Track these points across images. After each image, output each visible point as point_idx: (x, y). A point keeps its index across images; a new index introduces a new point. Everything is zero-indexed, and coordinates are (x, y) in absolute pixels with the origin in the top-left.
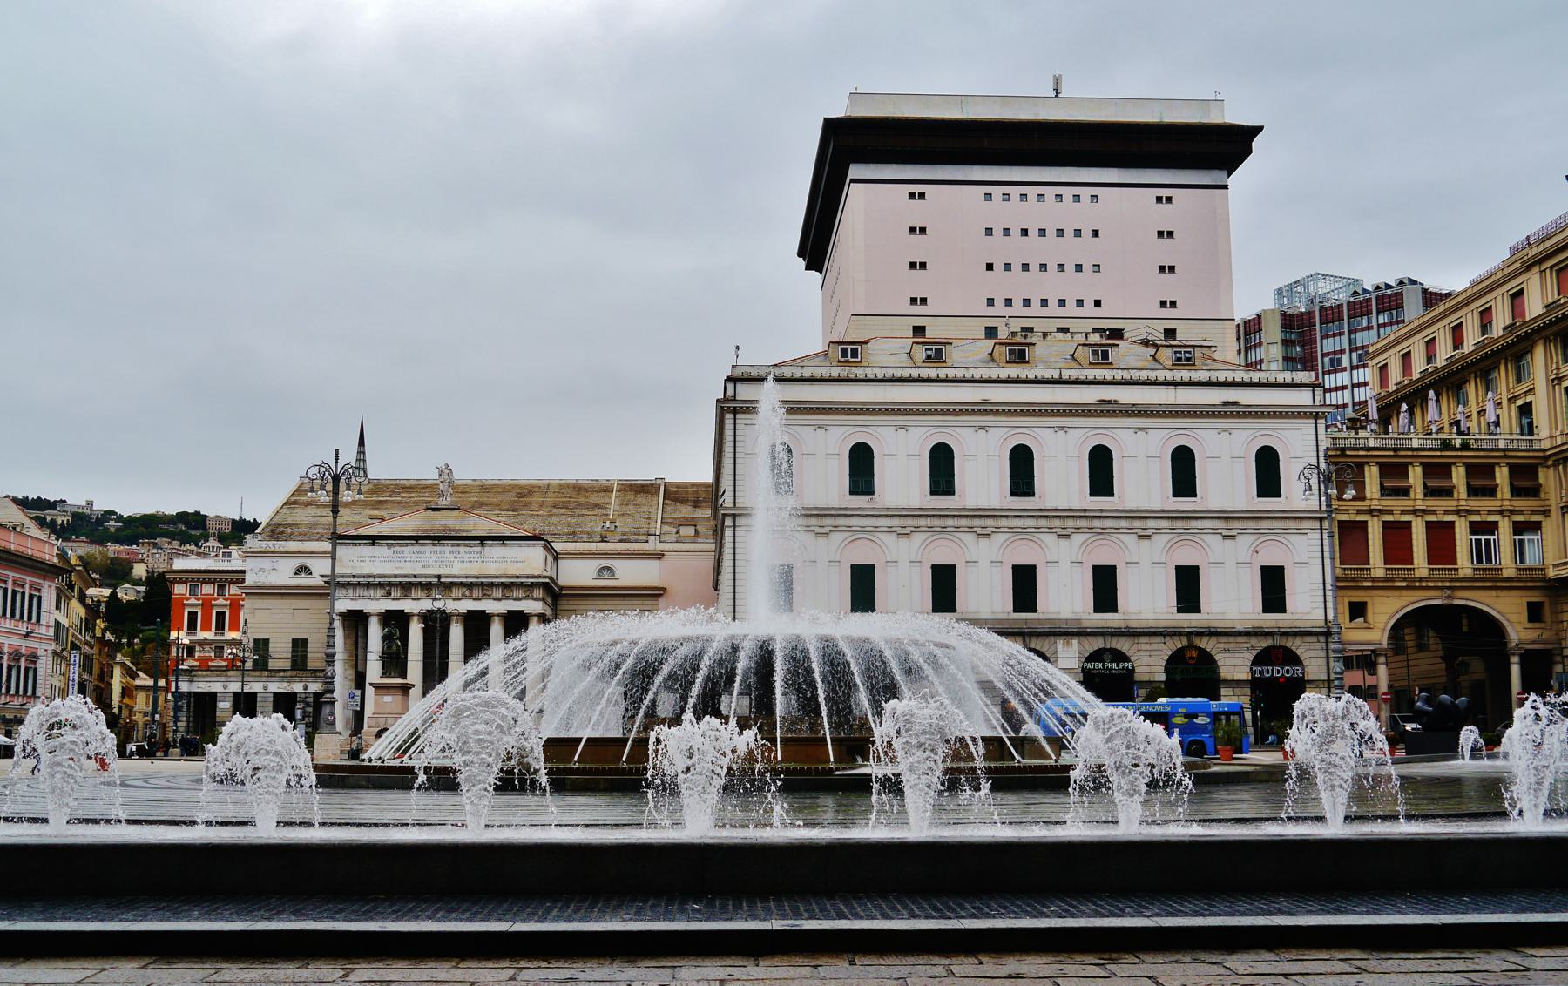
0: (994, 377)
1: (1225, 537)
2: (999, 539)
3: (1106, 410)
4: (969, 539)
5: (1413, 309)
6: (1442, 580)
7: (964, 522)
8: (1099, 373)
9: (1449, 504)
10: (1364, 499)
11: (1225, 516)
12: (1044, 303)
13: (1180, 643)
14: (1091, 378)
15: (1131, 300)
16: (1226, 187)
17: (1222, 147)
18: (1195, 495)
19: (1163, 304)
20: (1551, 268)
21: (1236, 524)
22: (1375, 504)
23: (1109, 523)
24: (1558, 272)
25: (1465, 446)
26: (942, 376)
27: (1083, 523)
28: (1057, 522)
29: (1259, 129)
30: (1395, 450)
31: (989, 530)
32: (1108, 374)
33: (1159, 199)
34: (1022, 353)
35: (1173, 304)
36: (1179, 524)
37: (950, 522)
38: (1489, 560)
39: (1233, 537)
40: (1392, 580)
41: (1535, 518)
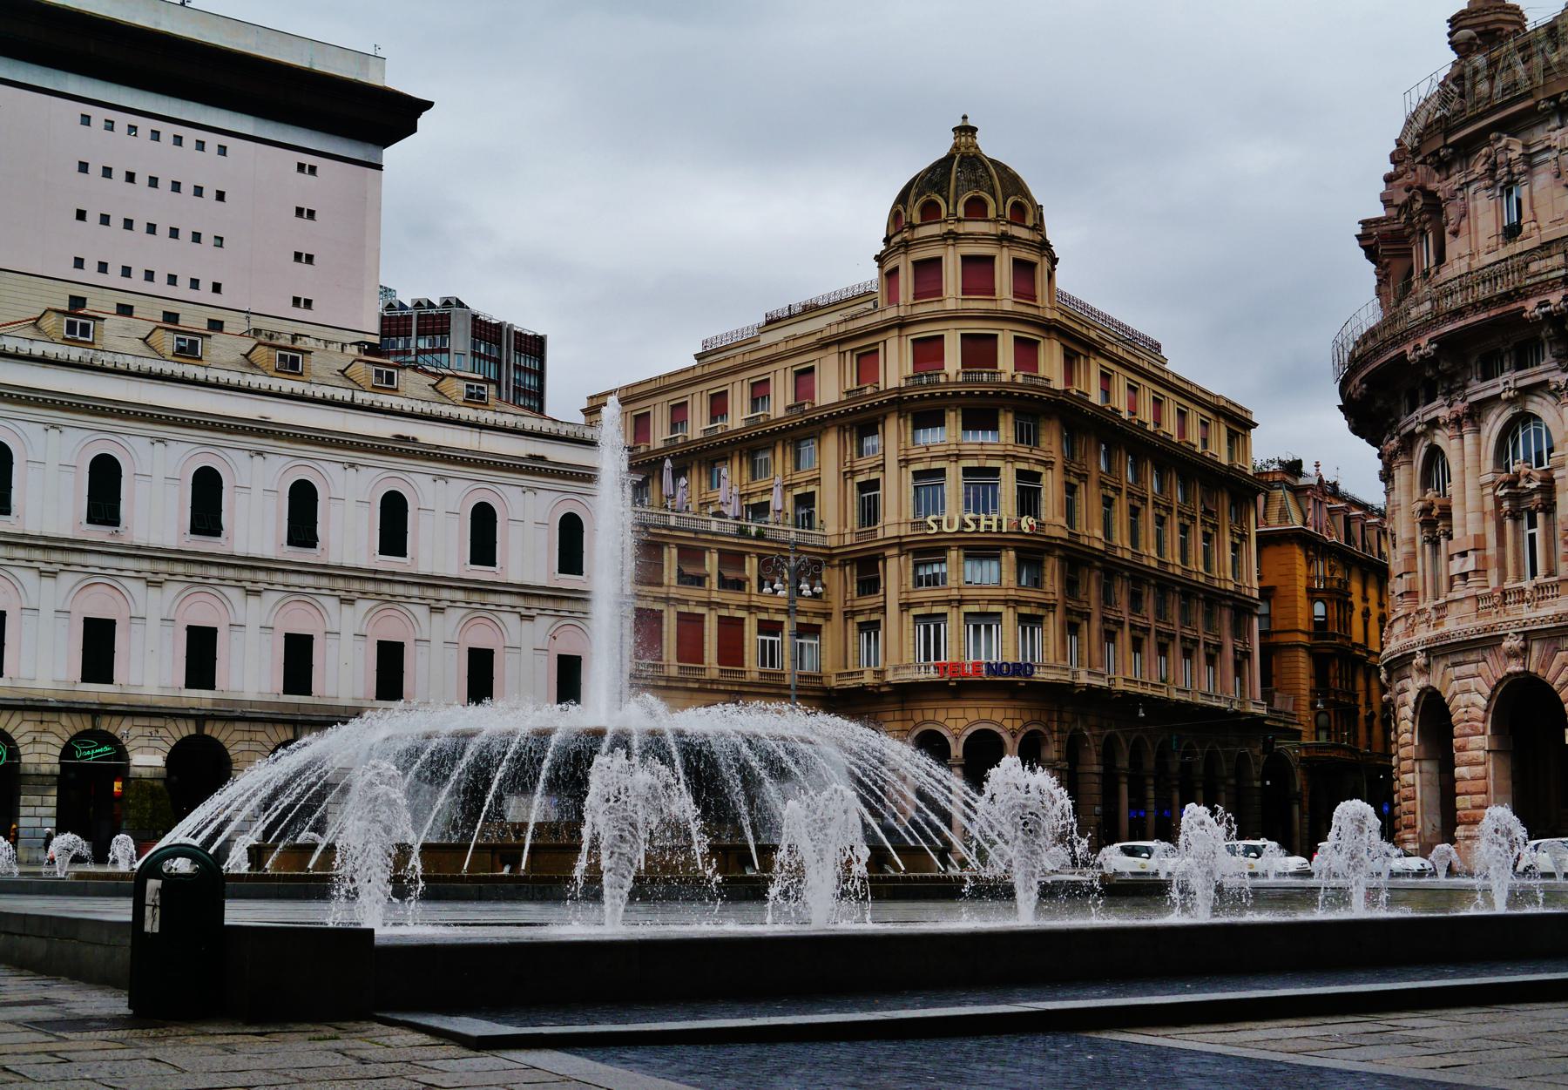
0: (275, 389)
1: (523, 617)
2: (271, 598)
3: (402, 448)
4: (235, 595)
5: (460, 339)
6: (732, 684)
7: (230, 573)
8: (287, 385)
9: (741, 598)
10: (661, 584)
11: (526, 592)
12: (172, 280)
13: (187, 729)
14: (387, 406)
15: (258, 288)
16: (379, 167)
17: (380, 117)
18: (493, 564)
19: (296, 301)
20: (852, 351)
21: (535, 603)
22: (675, 592)
23: (399, 590)
24: (859, 356)
25: (760, 535)
26: (212, 380)
27: (370, 587)
28: (340, 584)
29: (428, 105)
30: (696, 532)
31: (261, 586)
32: (298, 387)
33: (301, 167)
34: (295, 361)
35: (308, 303)
36: (476, 597)
37: (214, 571)
38: (772, 665)
39: (531, 618)
40: (686, 680)
41: (817, 621)
